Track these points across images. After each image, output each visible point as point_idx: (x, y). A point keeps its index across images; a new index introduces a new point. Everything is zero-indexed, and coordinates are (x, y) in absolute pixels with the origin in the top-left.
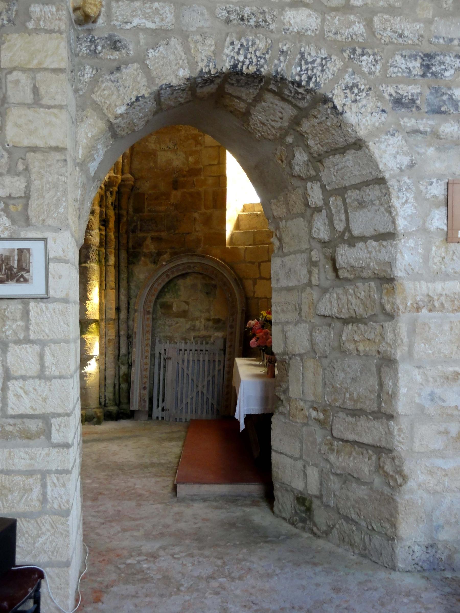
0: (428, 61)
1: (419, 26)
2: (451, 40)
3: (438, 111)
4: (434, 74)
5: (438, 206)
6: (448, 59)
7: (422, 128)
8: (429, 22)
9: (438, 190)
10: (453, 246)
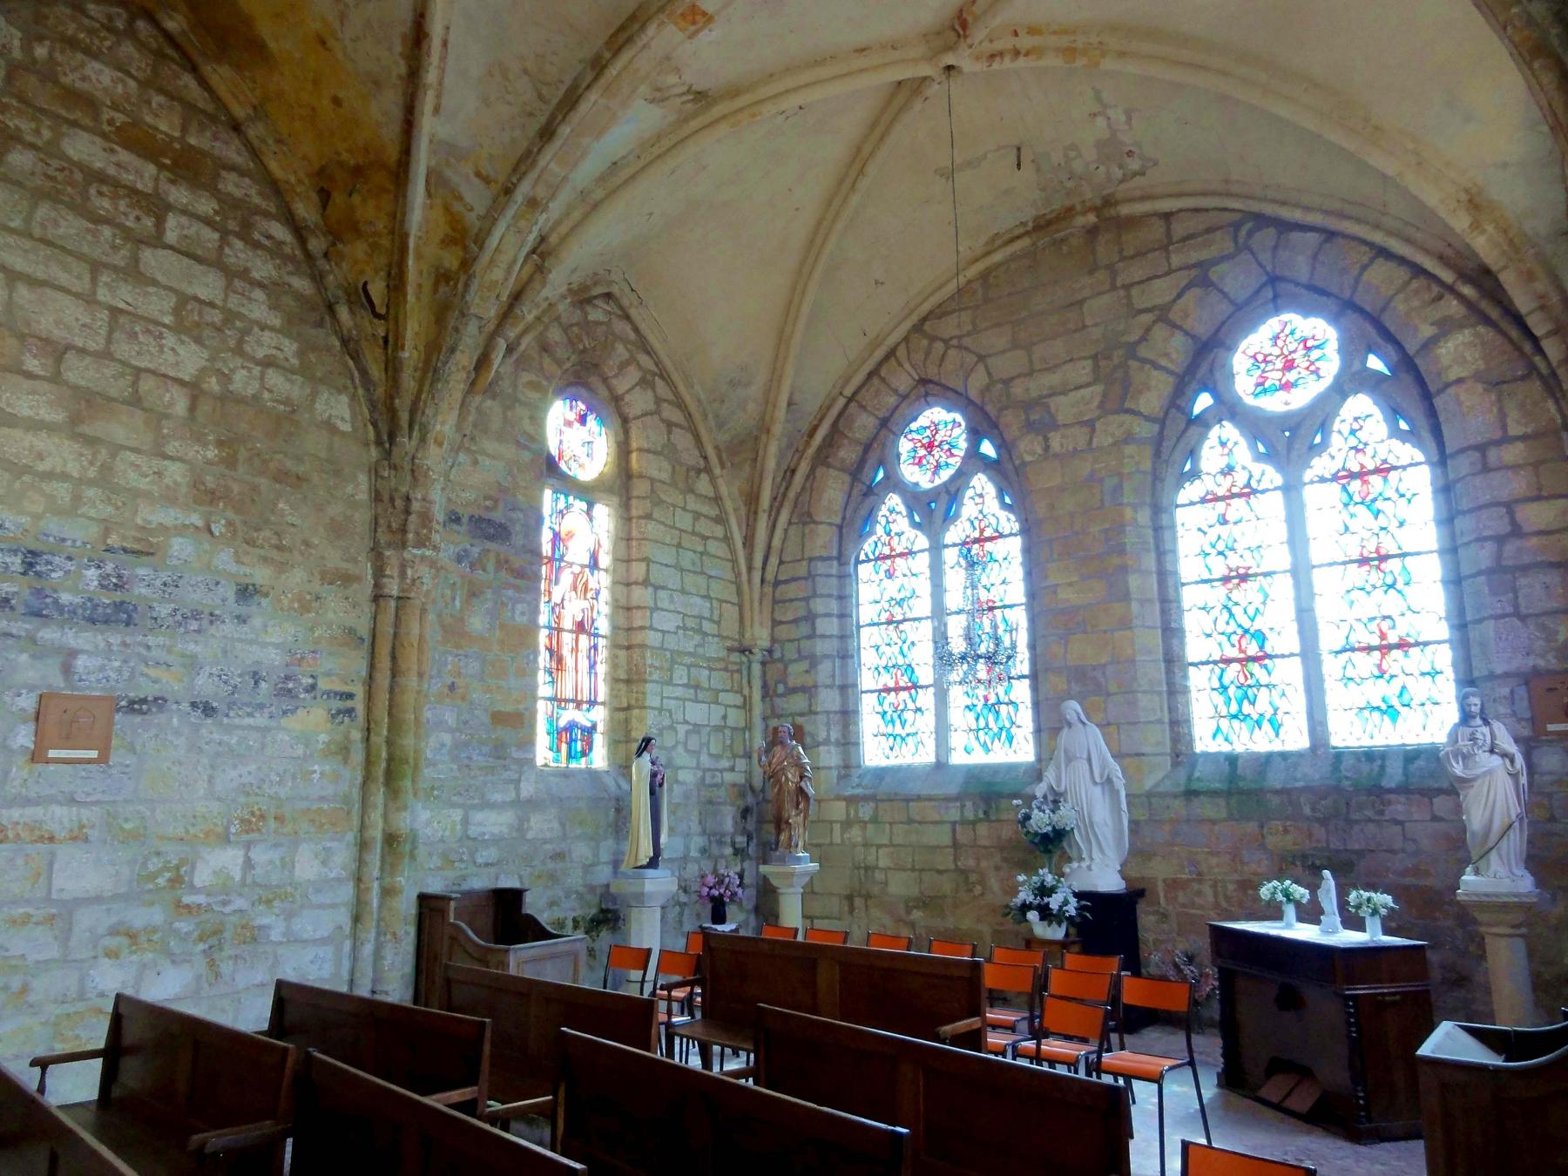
0: (31, 559)
1: (24, 520)
2: (64, 540)
3: (38, 614)
4: (38, 574)
5: (25, 722)
6: (57, 560)
7: (14, 631)
8: (37, 517)
9: (28, 702)
10: (39, 767)
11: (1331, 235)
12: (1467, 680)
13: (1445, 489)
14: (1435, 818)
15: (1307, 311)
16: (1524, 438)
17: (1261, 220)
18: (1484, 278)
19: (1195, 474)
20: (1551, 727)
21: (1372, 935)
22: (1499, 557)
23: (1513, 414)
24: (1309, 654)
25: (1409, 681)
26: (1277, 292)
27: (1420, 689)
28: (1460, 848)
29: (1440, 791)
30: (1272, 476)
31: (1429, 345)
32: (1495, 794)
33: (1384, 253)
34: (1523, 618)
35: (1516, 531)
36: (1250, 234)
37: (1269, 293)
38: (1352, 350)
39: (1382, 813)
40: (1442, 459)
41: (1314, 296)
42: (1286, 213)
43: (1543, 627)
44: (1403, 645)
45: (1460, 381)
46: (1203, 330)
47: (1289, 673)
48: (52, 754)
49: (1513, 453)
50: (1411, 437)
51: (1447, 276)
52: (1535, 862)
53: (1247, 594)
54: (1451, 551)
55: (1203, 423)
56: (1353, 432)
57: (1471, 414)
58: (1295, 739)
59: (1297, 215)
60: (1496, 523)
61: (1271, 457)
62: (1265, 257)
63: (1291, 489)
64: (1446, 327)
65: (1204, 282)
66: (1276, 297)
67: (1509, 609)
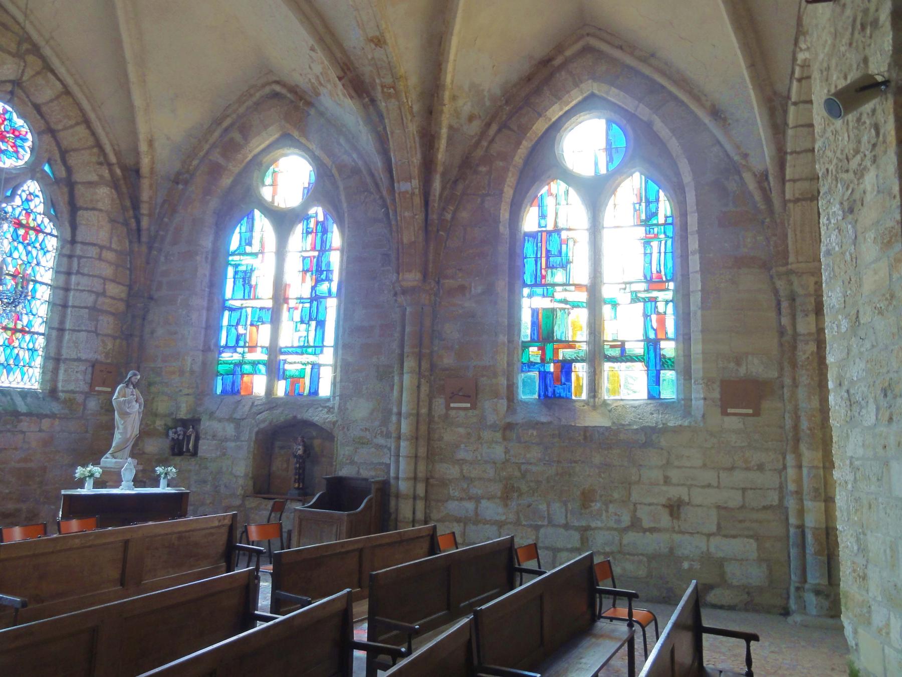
11: (67, 92)
14: (40, 431)
16: (116, 251)
17: (35, 49)
18: (133, 173)
20: (97, 388)
21: (163, 489)
22: (95, 302)
23: (115, 239)
25: (21, 353)
27: (25, 355)
29: (46, 416)
33: (87, 122)
34: (98, 335)
36: (28, 51)
37: (9, 87)
39: (16, 427)
42: (56, 63)
43: (103, 342)
44: (22, 331)
45: (101, 210)
49: (109, 255)
51: (113, 159)
56: (27, 200)
57: (97, 228)
59: (62, 71)
62: (29, 72)
66: (12, 93)
67: (93, 329)
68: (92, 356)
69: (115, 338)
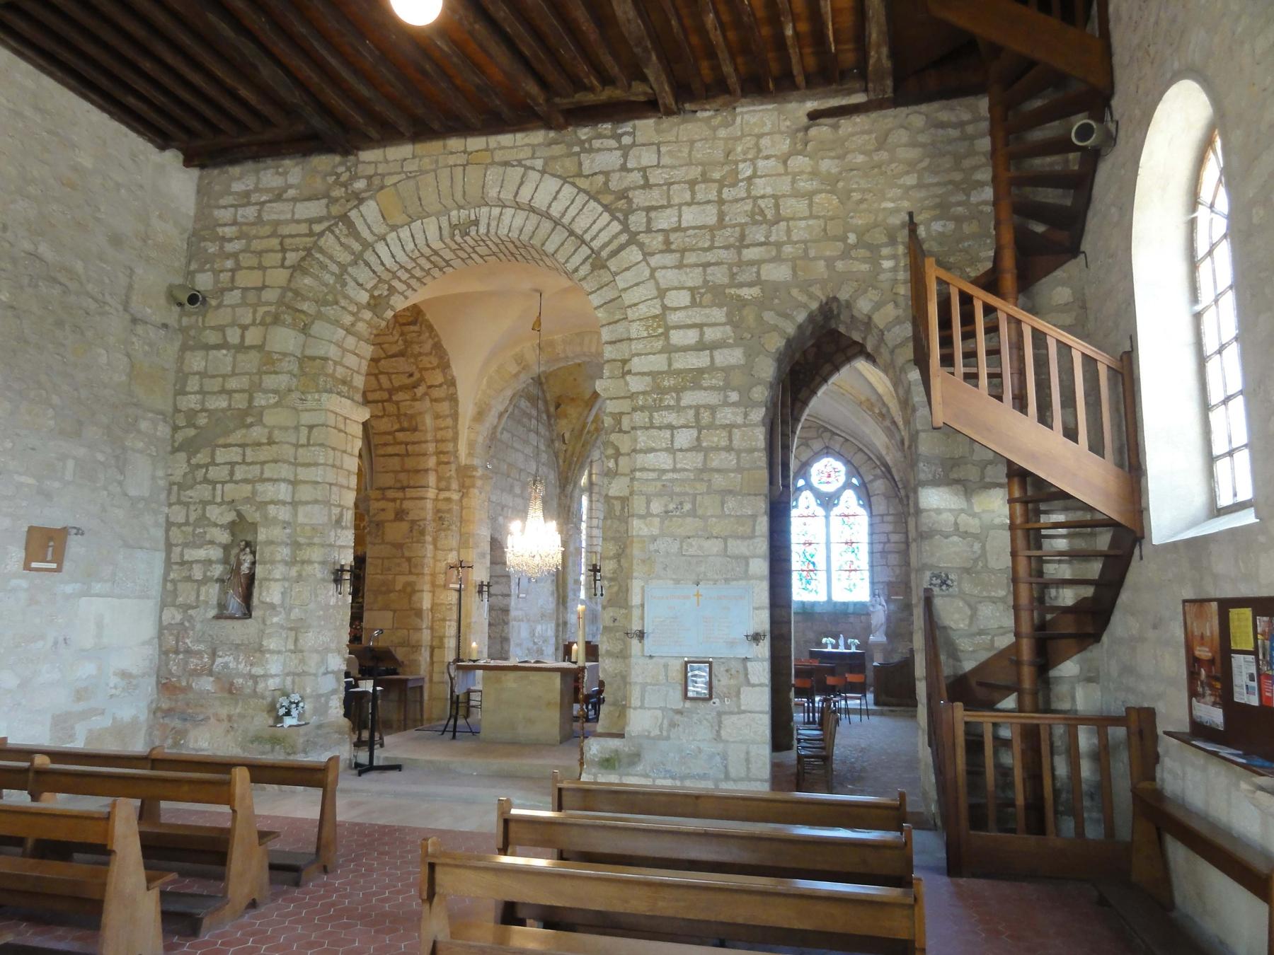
11: (847, 440)
12: (872, 583)
13: (871, 525)
15: (837, 459)
17: (826, 430)
18: (886, 465)
19: (796, 507)
21: (853, 650)
24: (828, 571)
26: (827, 451)
28: (868, 630)
30: (820, 511)
31: (871, 481)
32: (879, 616)
33: (861, 450)
35: (889, 541)
38: (849, 475)
40: (871, 515)
41: (839, 456)
46: (804, 460)
47: (821, 576)
48: (34, 565)
49: (889, 518)
50: (862, 506)
52: (887, 635)
53: (810, 550)
54: (871, 543)
55: (800, 490)
57: (881, 506)
58: (822, 597)
60: (884, 538)
61: (821, 505)
63: (827, 517)
64: (876, 477)
65: (808, 446)
68: (886, 579)
69: (900, 566)
